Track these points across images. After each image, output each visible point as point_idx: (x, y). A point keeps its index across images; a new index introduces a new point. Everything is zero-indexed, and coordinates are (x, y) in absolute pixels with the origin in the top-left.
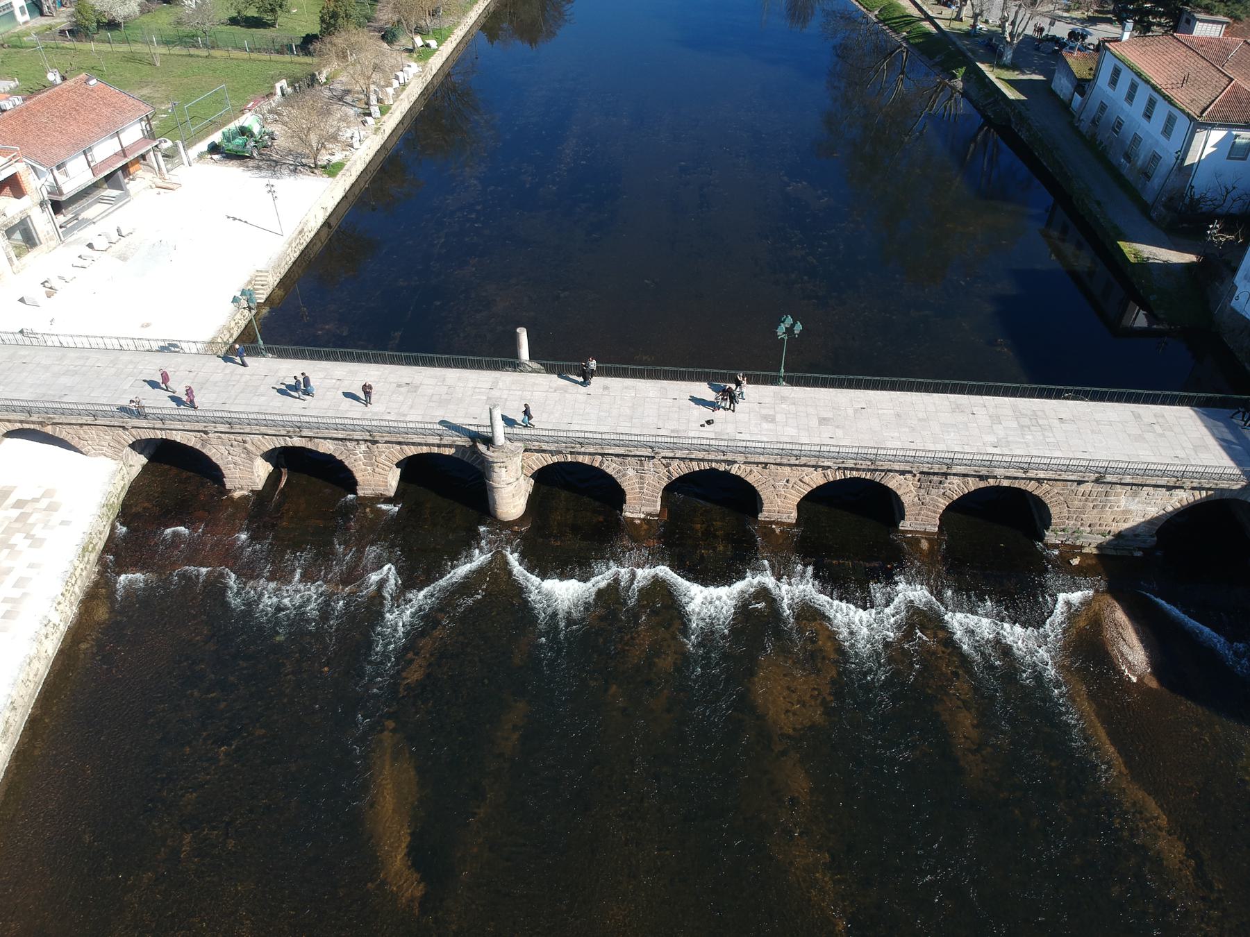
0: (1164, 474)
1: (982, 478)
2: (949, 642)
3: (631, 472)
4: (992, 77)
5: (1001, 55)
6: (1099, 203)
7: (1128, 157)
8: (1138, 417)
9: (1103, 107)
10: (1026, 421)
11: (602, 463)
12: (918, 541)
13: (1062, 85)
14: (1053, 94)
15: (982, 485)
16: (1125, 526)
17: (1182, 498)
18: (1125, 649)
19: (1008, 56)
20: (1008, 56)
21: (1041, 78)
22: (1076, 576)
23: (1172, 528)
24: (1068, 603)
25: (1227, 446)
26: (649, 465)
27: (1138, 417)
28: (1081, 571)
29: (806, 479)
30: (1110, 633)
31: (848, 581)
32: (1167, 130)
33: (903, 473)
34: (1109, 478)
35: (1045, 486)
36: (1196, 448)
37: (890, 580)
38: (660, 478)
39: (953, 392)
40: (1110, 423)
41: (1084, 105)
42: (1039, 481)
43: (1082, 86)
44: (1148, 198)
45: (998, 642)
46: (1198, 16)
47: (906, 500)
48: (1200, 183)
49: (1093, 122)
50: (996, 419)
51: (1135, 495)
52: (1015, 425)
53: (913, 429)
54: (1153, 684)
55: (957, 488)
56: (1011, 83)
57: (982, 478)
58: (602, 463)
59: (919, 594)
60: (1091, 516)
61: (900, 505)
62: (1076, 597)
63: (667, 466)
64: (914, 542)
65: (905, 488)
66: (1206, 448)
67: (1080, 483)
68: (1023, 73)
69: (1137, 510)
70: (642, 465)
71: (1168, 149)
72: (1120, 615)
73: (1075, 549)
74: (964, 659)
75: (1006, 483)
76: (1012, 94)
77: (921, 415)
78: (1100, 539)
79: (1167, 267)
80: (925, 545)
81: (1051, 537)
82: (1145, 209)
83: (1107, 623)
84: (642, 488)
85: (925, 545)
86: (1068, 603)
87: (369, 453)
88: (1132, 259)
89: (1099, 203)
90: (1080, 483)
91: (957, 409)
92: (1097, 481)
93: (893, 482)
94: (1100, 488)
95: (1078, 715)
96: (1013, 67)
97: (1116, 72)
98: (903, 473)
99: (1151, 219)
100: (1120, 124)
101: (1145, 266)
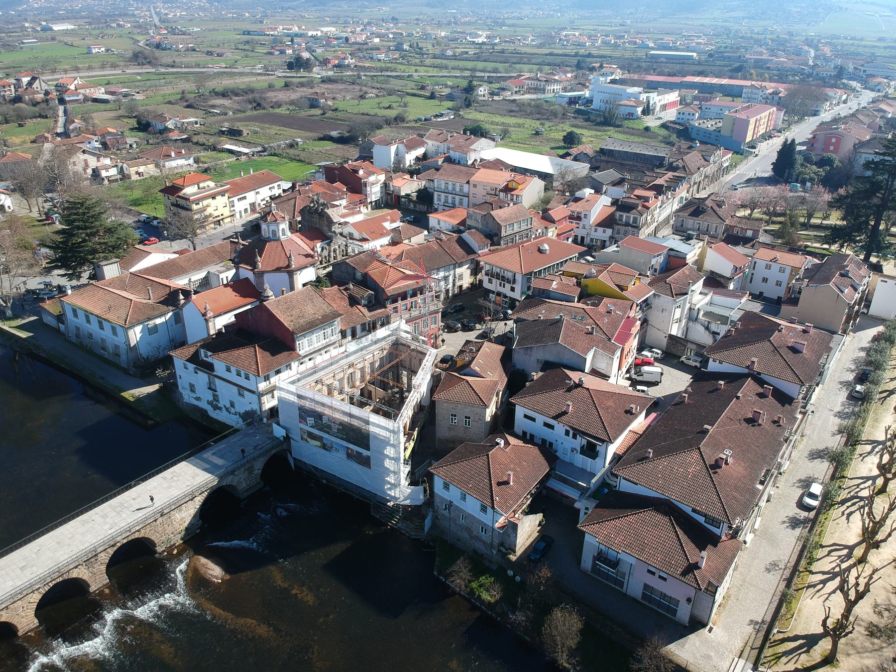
0: (185, 496)
1: (113, 546)
2: (141, 622)
4: (6, 328)
5: (4, 313)
6: (102, 378)
7: (104, 349)
8: (164, 478)
9: (78, 329)
10: (119, 509)
12: (103, 591)
13: (48, 320)
14: (47, 326)
15: (115, 548)
16: (186, 524)
17: (199, 501)
18: (211, 572)
19: (9, 313)
20: (9, 313)
21: (35, 318)
22: (178, 558)
23: (204, 512)
24: (181, 571)
25: (205, 470)
27: (164, 478)
28: (180, 554)
30: (202, 571)
31: (78, 632)
32: (115, 332)
33: (76, 567)
34: (166, 511)
35: (142, 531)
36: (193, 478)
37: (100, 617)
39: (78, 516)
40: (155, 488)
41: (67, 328)
42: (138, 531)
43: (60, 318)
44: (124, 365)
45: (161, 607)
46: (101, 264)
47: (85, 578)
48: (144, 351)
49: (77, 336)
50: (105, 516)
51: (181, 510)
52: (115, 513)
53: (69, 545)
54: (228, 577)
55: (105, 558)
56: (20, 327)
57: (113, 546)
59: (117, 613)
60: (169, 530)
61: (84, 581)
62: (183, 566)
64: (101, 592)
65: (82, 573)
66: (197, 475)
67: (155, 521)
68: (24, 319)
69: (186, 515)
71: (119, 340)
72: (203, 560)
73: (172, 548)
74: (151, 625)
75: (125, 541)
76: (23, 335)
77: (69, 536)
78: (180, 536)
79: (149, 395)
80: (107, 591)
81: (159, 549)
82: (125, 371)
83: (200, 567)
85: (107, 591)
86: (181, 571)
88: (131, 399)
89: (102, 378)
90: (155, 521)
91: (84, 523)
92: (162, 516)
93: (74, 574)
95: (212, 611)
96: (15, 317)
97: (74, 311)
98: (76, 567)
99: (130, 375)
100: (91, 335)
101: (139, 400)
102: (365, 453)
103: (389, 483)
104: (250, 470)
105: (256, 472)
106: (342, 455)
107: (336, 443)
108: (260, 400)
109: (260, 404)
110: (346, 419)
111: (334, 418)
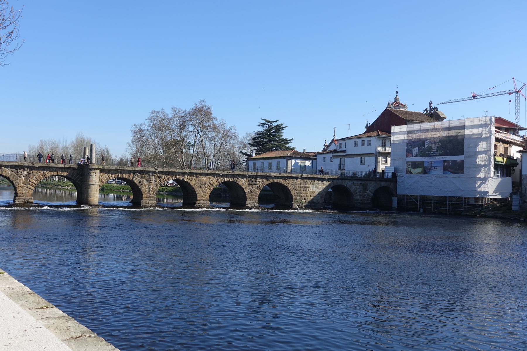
3: (145, 182)
11: (133, 177)
26: (153, 178)
29: (212, 182)
38: (157, 185)
47: (247, 190)
58: (133, 177)
63: (160, 177)
70: (150, 178)
84: (149, 191)
87: (28, 175)
94: (303, 181)
102: (458, 158)
103: (480, 179)
104: (365, 188)
105: (368, 192)
106: (439, 171)
107: (435, 162)
108: (376, 159)
109: (377, 162)
110: (445, 134)
111: (434, 138)
